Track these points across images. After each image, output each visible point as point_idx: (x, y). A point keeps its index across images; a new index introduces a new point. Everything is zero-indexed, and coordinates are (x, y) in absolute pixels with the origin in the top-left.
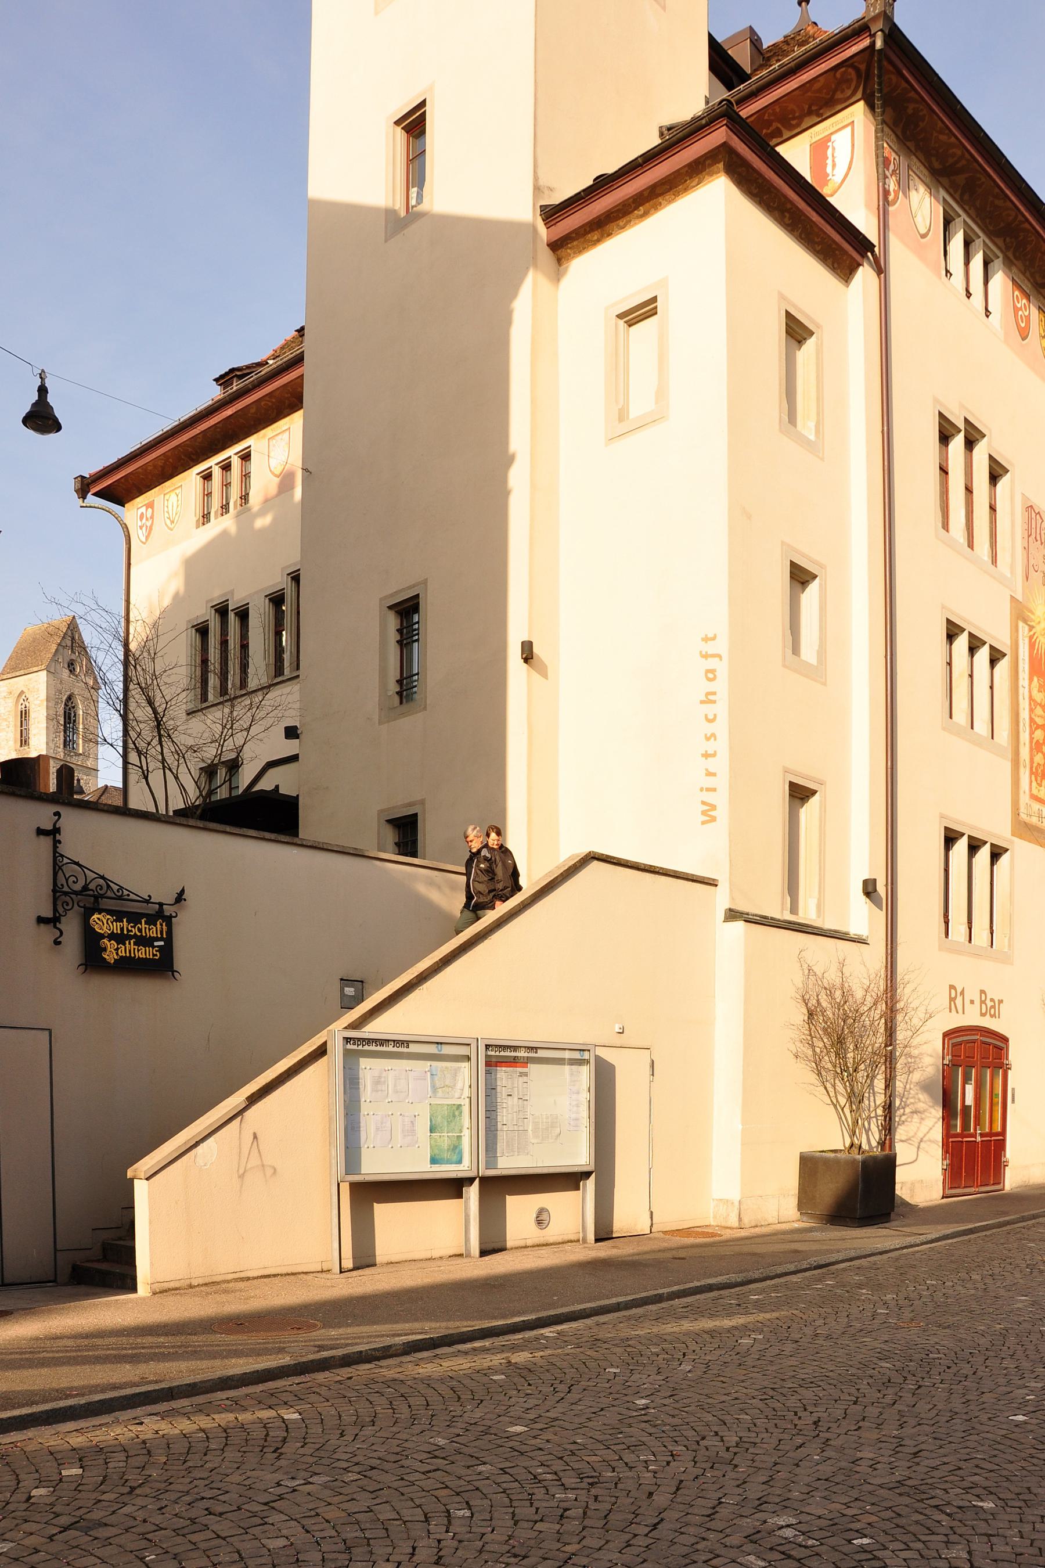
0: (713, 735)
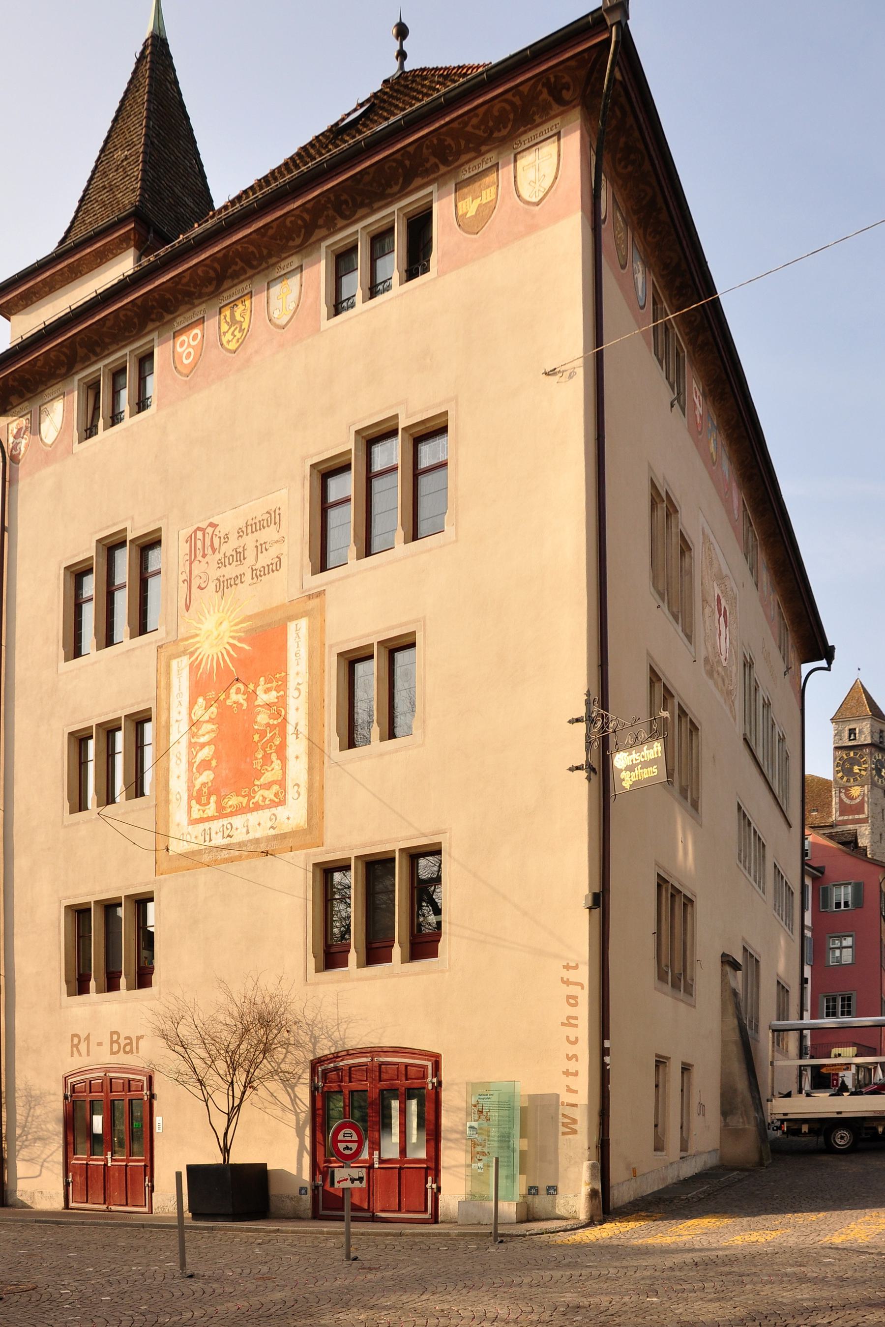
0: (575, 1057)
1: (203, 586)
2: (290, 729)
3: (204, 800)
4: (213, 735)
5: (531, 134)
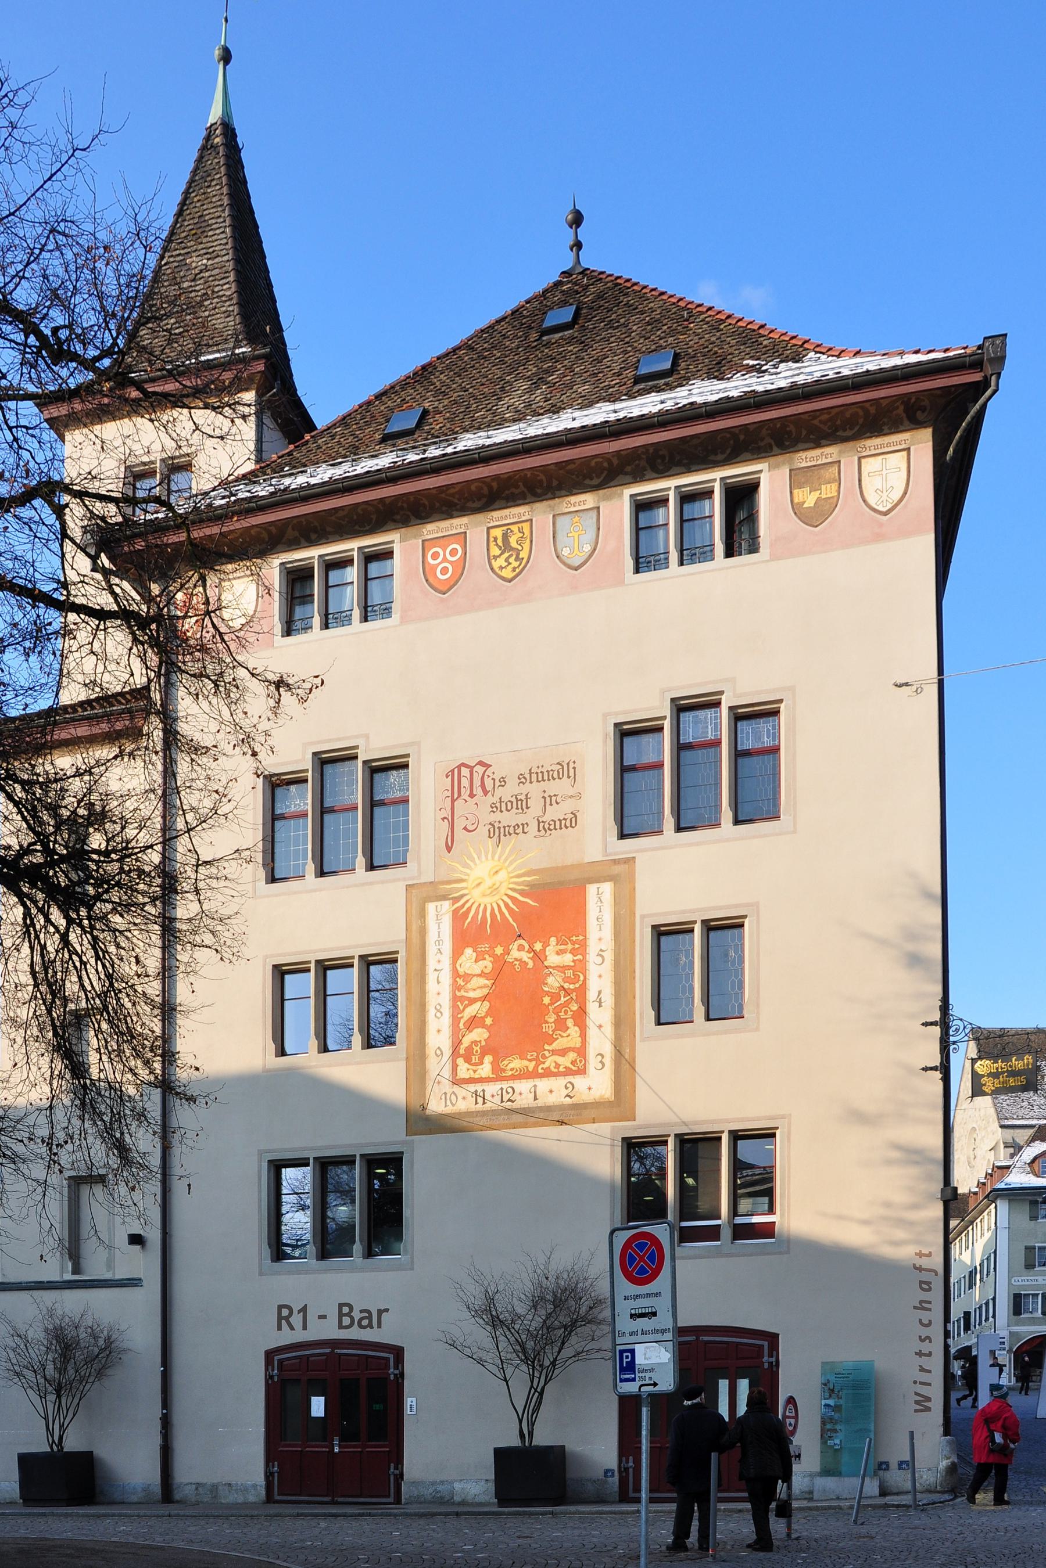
0: (928, 1338)
1: (470, 828)
2: (591, 995)
3: (475, 1059)
4: (486, 991)
5: (878, 441)
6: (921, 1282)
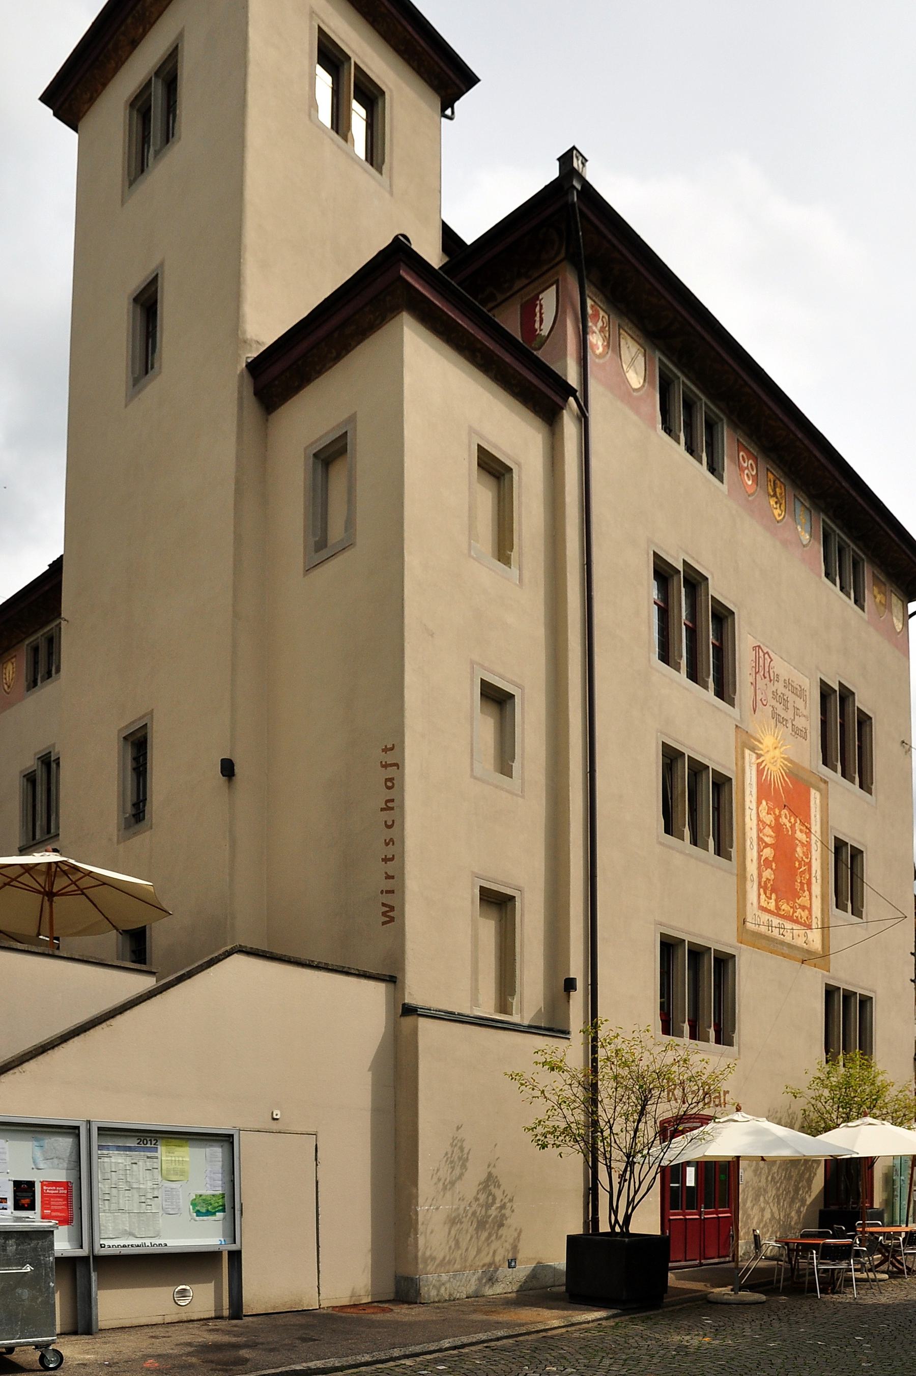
0: (392, 840)
6: (387, 780)
